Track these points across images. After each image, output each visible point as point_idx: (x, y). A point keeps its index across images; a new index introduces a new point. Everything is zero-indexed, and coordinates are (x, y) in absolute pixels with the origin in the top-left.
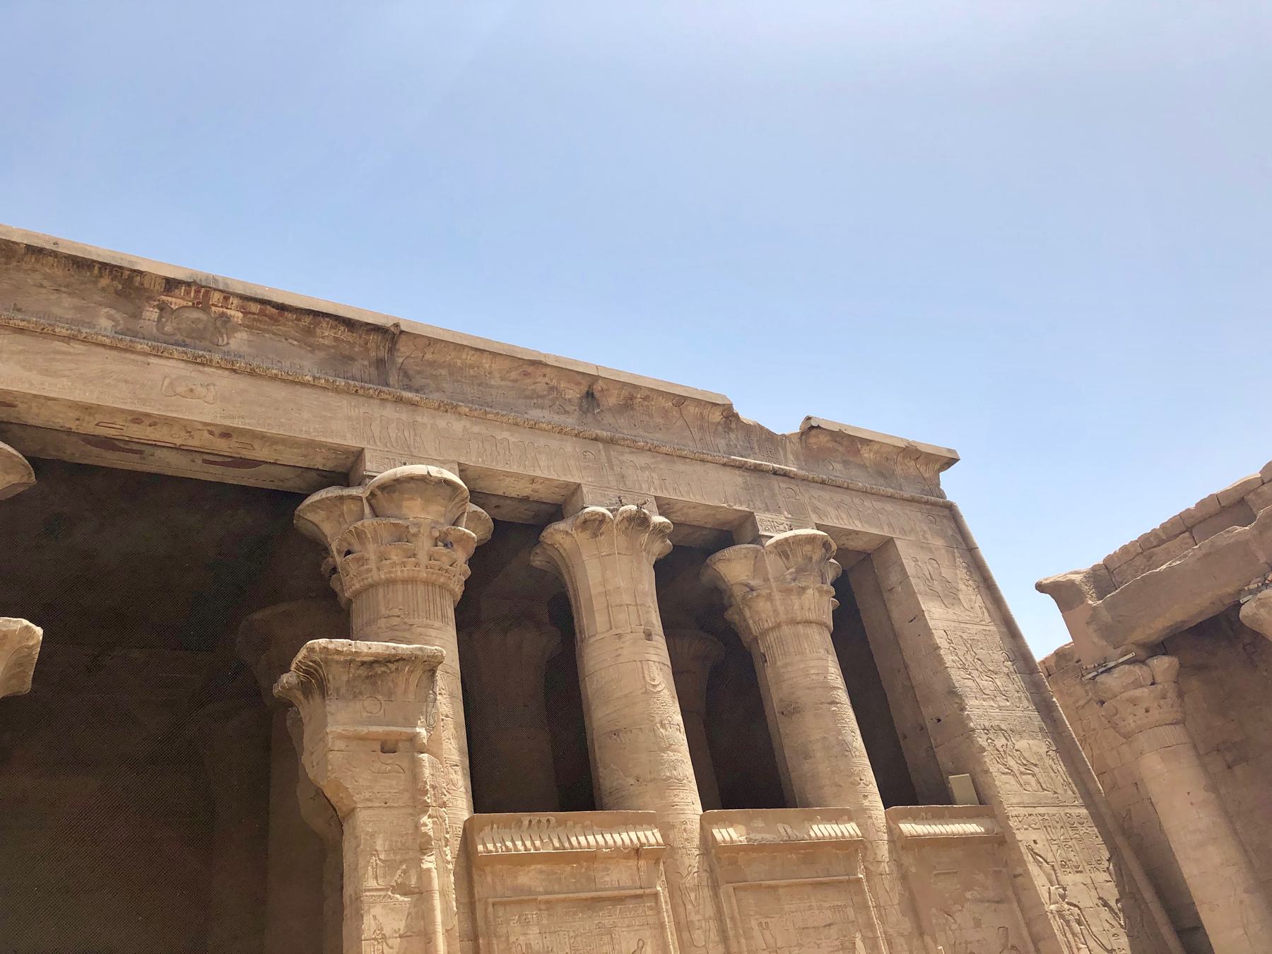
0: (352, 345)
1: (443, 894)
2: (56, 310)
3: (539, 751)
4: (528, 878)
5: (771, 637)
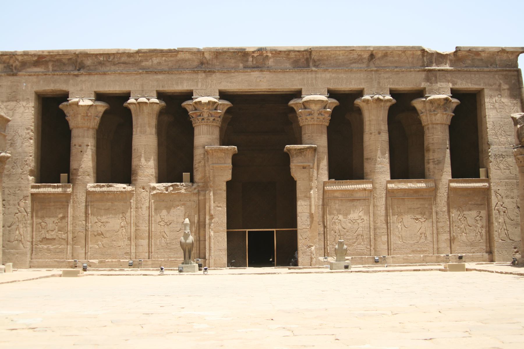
0: (299, 56)
1: (315, 198)
2: (231, 64)
3: (346, 164)
4: (336, 194)
5: (427, 127)
